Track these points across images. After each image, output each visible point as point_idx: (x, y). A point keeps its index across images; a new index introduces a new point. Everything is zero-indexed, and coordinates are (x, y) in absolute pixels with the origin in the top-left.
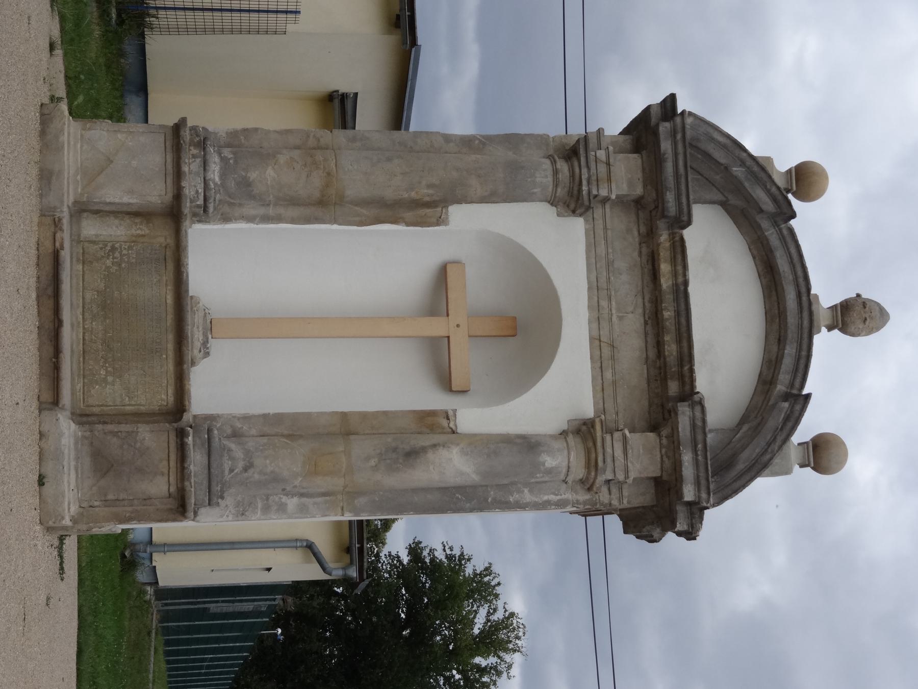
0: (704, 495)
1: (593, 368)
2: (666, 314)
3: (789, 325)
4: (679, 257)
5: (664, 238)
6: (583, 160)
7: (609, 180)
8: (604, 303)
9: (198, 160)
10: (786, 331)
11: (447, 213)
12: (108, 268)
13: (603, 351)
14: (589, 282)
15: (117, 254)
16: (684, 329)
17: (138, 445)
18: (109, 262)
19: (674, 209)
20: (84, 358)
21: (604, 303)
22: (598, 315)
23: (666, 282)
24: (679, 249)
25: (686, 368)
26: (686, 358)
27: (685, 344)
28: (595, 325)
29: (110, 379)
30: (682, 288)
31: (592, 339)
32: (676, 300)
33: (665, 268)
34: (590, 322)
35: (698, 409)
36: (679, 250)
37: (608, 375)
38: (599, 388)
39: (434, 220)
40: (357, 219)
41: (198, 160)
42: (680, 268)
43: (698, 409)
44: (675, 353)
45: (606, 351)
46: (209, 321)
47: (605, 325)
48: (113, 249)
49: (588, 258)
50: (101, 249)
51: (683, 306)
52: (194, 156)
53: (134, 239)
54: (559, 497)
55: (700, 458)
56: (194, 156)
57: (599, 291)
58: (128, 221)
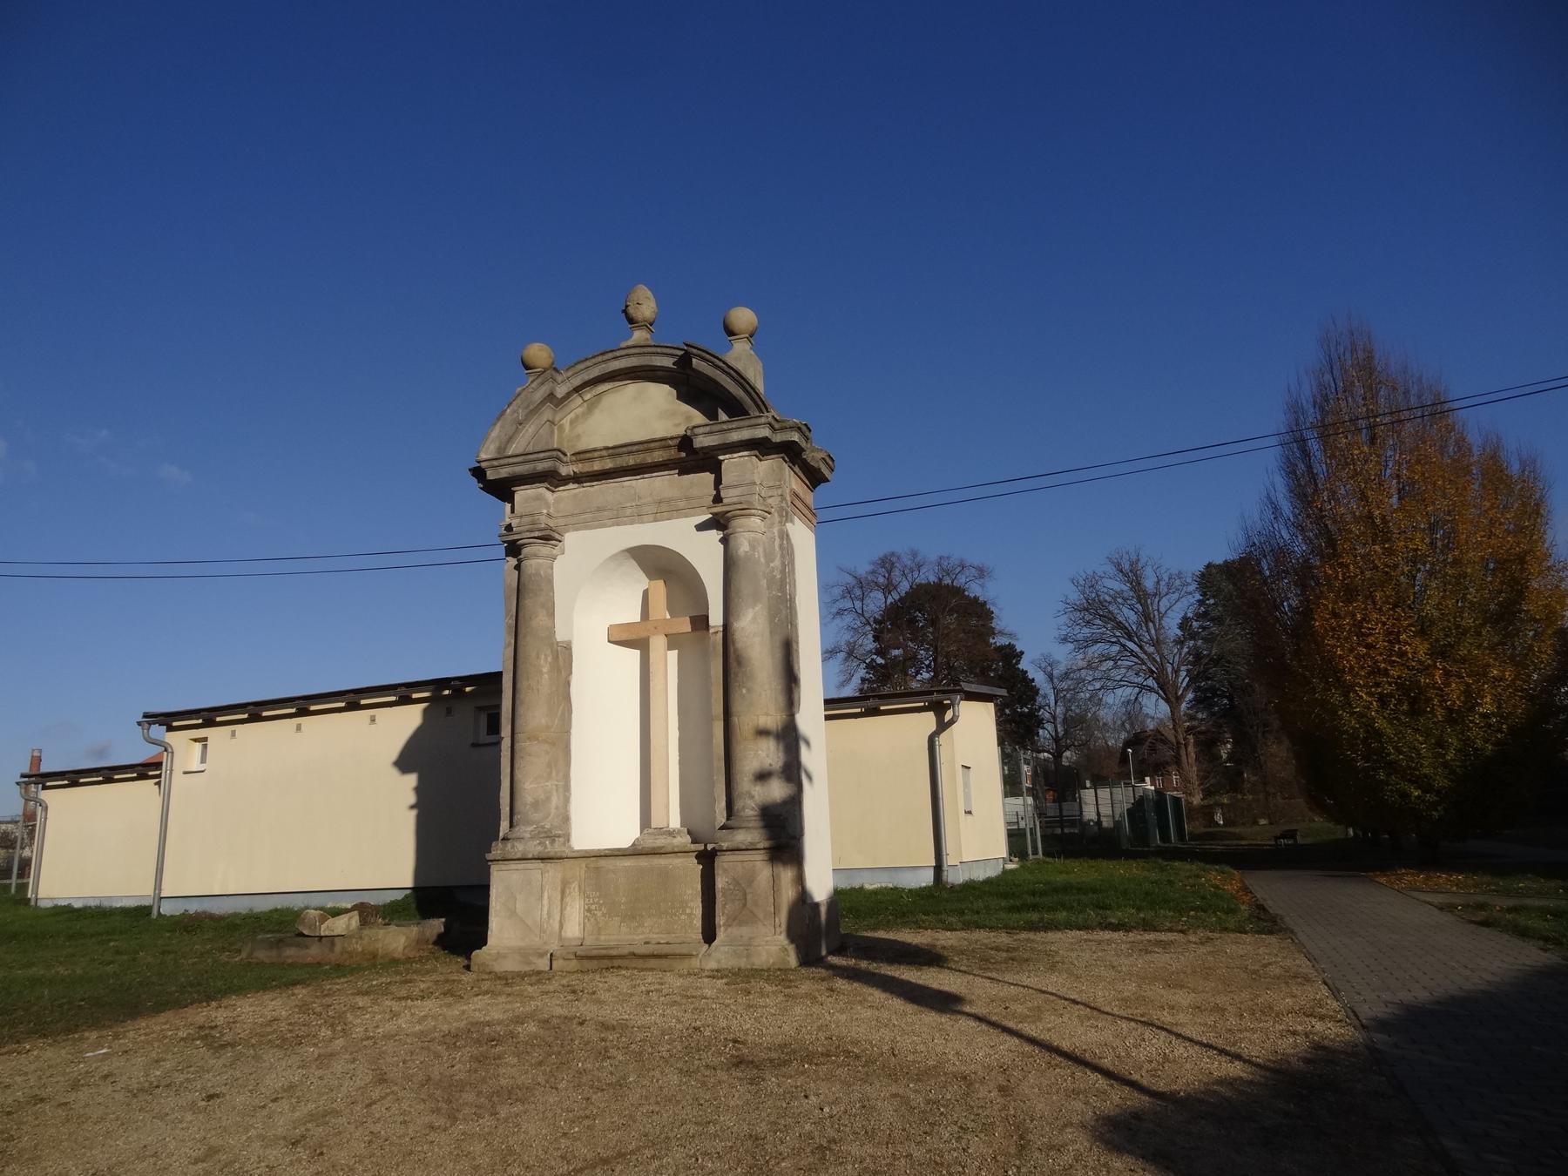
0: (763, 420)
2: (632, 462)
8: (629, 512)
13: (666, 510)
16: (641, 447)
21: (629, 512)
22: (638, 517)
23: (609, 464)
33: (597, 466)
35: (696, 431)
37: (682, 504)
42: (596, 454)
43: (696, 431)
45: (664, 507)
48: (589, 910)
57: (617, 516)
58: (568, 899)
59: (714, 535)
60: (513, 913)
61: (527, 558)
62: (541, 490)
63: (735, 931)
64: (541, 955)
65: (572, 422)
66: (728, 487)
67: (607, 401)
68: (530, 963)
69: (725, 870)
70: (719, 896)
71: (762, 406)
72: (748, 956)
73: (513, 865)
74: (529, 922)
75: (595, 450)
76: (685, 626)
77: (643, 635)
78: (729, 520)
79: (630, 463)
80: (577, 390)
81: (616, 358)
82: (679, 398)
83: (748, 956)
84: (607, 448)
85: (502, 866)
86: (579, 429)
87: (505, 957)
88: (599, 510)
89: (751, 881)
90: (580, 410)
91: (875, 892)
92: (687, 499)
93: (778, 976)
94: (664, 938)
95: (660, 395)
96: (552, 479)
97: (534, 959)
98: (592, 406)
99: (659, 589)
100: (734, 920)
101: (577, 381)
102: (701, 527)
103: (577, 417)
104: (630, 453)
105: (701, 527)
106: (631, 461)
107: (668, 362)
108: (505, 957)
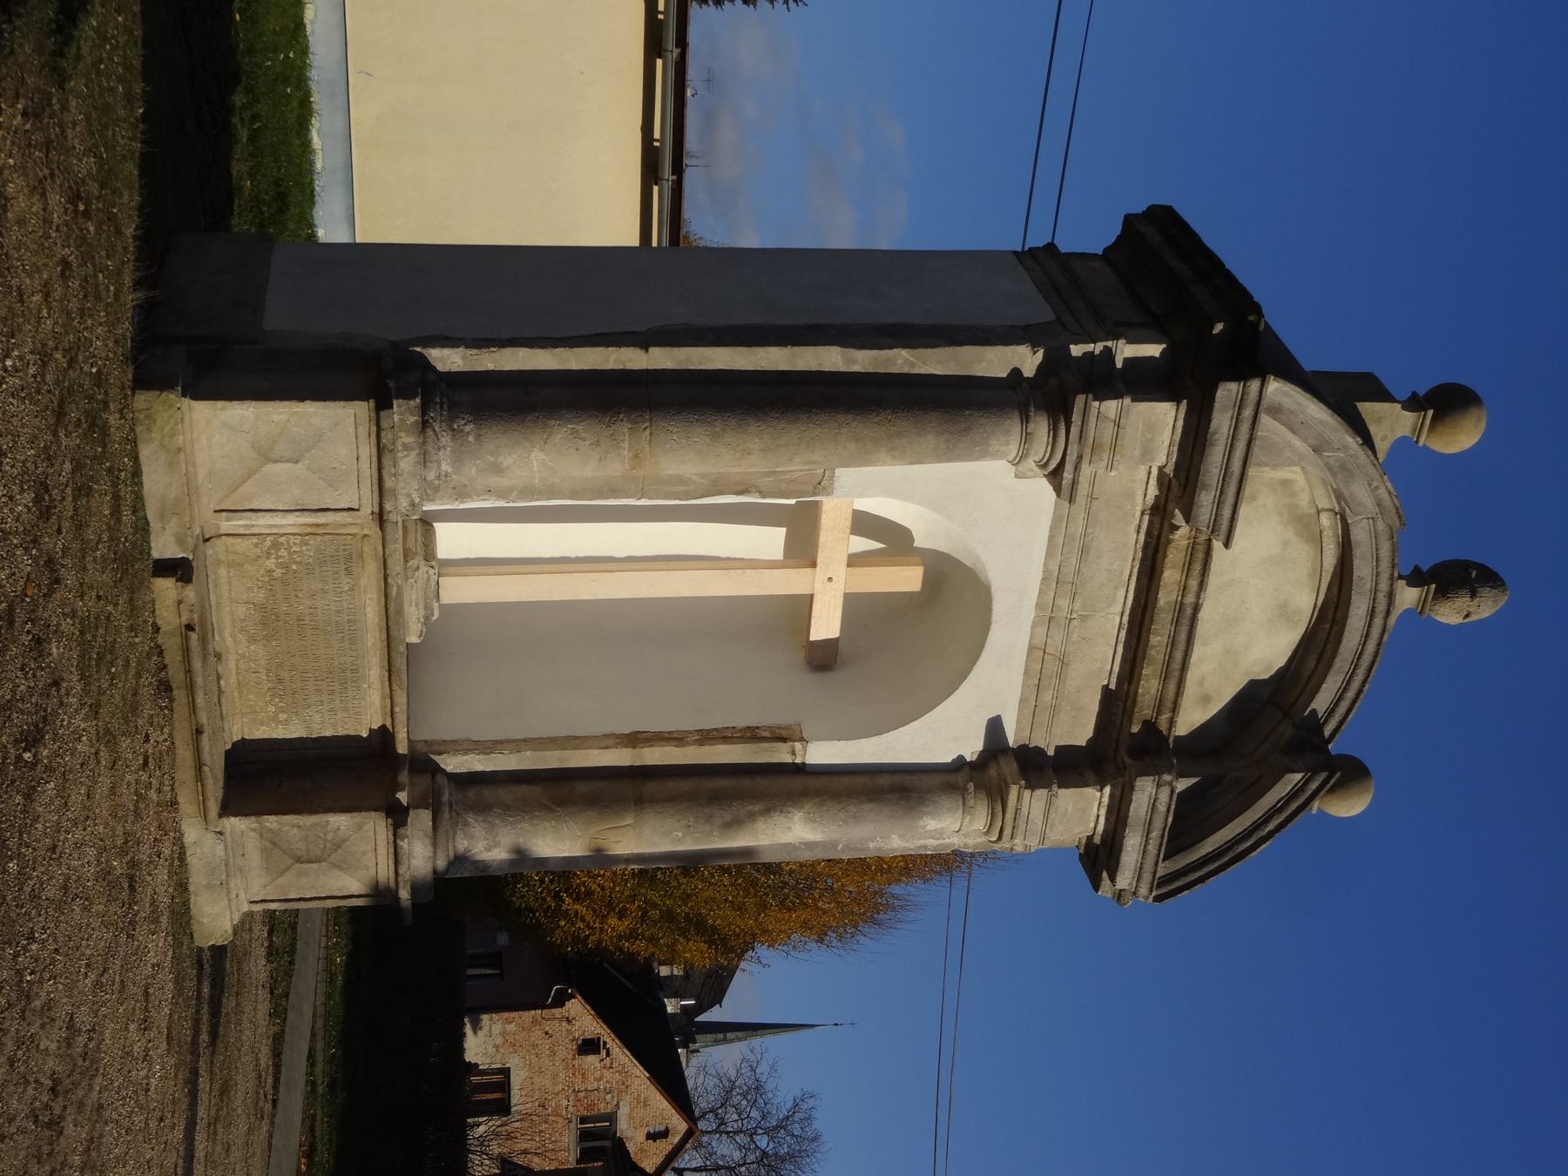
0: (1143, 891)
1: (1024, 685)
2: (1154, 640)
3: (1342, 649)
4: (1197, 567)
5: (1182, 535)
6: (1075, 430)
7: (1114, 448)
8: (1064, 603)
9: (413, 454)
10: (1333, 657)
11: (832, 478)
12: (270, 571)
13: (1045, 667)
14: (1046, 571)
15: (283, 552)
16: (1176, 666)
17: (330, 837)
18: (270, 563)
19: (1207, 517)
20: (240, 693)
21: (1064, 603)
22: (1047, 617)
23: (1166, 596)
24: (1199, 559)
25: (1165, 717)
26: (1169, 704)
27: (1172, 687)
28: (1042, 630)
29: (282, 717)
30: (1189, 611)
31: (1032, 648)
32: (1177, 622)
33: (1171, 576)
34: (1034, 625)
36: (1200, 556)
37: (1047, 697)
38: (1029, 712)
39: (811, 488)
40: (683, 488)
41: (413, 454)
42: (1193, 584)
44: (1153, 691)
45: (1051, 666)
46: (433, 584)
47: (1058, 635)
48: (276, 545)
49: (1051, 538)
50: (256, 545)
51: (1183, 637)
52: (406, 447)
53: (309, 530)
54: (937, 842)
55: (1150, 847)
56: (406, 447)
59: (972, 748)
60: (267, 456)
61: (1027, 437)
63: (252, 844)
64: (180, 541)
65: (1286, 483)
66: (1049, 804)
67: (1302, 555)
68: (162, 517)
69: (360, 827)
70: (307, 820)
72: (209, 887)
73: (367, 451)
74: (248, 487)
75: (1202, 585)
76: (826, 625)
77: (821, 558)
78: (992, 799)
79: (1155, 619)
81: (1372, 613)
82: (1253, 687)
83: (209, 887)
84: (1197, 608)
87: (172, 465)
88: (1084, 550)
90: (1304, 500)
91: (306, 144)
92: (1054, 709)
93: (182, 917)
94: (230, 682)
96: (1180, 487)
97: (172, 525)
98: (1305, 525)
99: (908, 579)
100: (273, 844)
101: (1360, 535)
102: (995, 727)
103: (1294, 494)
104: (1173, 643)
105: (995, 727)
106: (1158, 639)
107: (1321, 703)
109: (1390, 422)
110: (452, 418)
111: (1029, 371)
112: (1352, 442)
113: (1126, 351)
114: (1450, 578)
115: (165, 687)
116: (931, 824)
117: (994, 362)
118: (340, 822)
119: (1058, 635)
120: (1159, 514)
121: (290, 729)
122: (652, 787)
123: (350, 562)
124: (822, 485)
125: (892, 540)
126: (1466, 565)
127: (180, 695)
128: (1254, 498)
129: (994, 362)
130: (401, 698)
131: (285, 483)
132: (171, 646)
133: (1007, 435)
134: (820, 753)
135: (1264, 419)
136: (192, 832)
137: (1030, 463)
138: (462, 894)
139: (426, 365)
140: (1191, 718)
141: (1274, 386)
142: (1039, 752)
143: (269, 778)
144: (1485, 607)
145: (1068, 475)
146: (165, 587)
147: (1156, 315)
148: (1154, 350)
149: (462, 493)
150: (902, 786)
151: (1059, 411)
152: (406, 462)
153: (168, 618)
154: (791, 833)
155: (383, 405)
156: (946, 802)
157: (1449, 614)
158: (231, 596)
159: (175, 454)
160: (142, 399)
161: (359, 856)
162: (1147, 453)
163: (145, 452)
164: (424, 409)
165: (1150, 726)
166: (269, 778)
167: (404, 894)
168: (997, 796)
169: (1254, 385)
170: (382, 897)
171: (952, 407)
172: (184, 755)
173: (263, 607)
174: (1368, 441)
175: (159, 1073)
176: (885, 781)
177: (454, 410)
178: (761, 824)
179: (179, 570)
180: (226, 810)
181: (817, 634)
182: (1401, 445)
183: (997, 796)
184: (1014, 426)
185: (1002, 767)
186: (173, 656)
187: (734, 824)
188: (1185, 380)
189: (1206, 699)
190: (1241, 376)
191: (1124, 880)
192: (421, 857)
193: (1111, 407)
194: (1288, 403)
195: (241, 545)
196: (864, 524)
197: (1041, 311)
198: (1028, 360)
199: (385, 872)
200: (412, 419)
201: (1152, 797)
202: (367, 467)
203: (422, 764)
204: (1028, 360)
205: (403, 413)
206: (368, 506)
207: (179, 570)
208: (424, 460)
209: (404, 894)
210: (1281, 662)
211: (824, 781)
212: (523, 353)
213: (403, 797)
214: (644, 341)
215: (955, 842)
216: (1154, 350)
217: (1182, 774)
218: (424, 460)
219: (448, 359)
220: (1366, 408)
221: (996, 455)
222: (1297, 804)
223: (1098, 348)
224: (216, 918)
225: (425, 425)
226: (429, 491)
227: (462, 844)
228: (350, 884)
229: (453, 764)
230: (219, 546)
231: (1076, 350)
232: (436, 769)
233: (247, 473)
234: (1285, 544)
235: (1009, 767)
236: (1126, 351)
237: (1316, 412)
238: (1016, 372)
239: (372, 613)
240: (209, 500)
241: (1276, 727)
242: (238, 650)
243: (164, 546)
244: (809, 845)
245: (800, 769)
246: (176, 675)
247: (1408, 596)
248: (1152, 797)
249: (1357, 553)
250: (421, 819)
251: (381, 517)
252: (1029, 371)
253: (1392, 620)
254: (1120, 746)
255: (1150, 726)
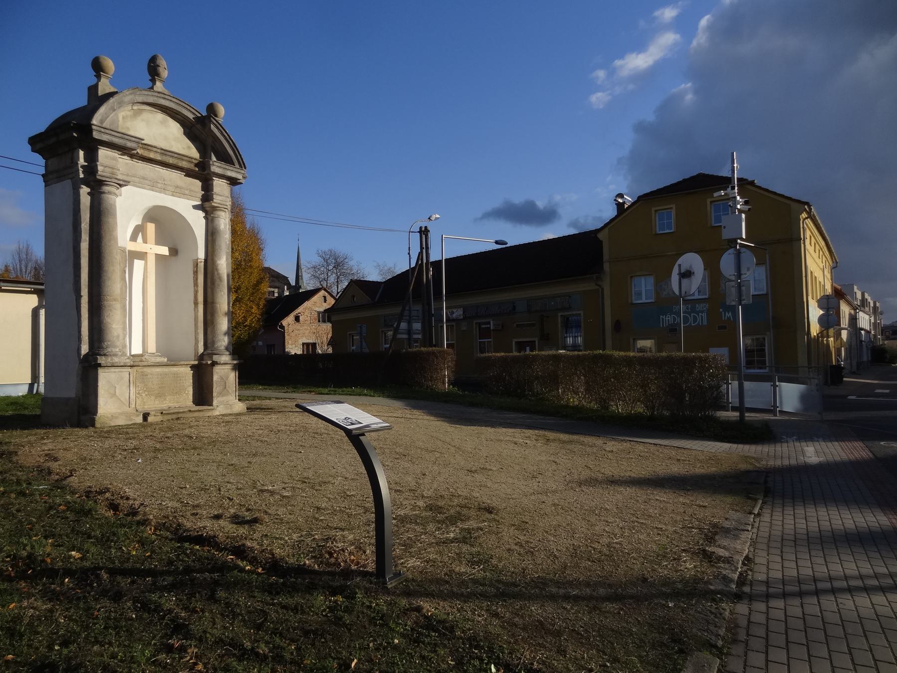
2: (171, 162)
5: (140, 151)
8: (159, 185)
13: (178, 192)
21: (159, 185)
22: (164, 190)
24: (147, 147)
37: (187, 192)
45: (178, 190)
57: (153, 185)
59: (201, 214)
60: (114, 395)
61: (110, 193)
62: (115, 154)
63: (221, 399)
64: (138, 416)
65: (123, 118)
67: (145, 115)
68: (131, 420)
71: (242, 165)
73: (113, 369)
76: (164, 251)
79: (166, 161)
80: (134, 103)
81: (164, 98)
82: (185, 133)
85: (106, 370)
86: (129, 124)
87: (116, 418)
88: (144, 178)
89: (227, 378)
90: (129, 113)
94: (177, 405)
95: (175, 128)
96: (124, 150)
99: (151, 228)
100: (220, 394)
101: (140, 99)
102: (195, 207)
105: (195, 207)
106: (171, 161)
107: (191, 116)
108: (116, 418)
109: (105, 86)
110: (103, 348)
111: (89, 190)
112: (112, 100)
113: (82, 161)
114: (153, 71)
115: (178, 419)
116: (222, 227)
117: (85, 199)
118: (215, 378)
119: (169, 188)
120: (132, 156)
121: (190, 390)
122: (209, 300)
123: (144, 375)
124: (123, 250)
125: (139, 230)
126: (149, 67)
127: (180, 415)
128: (128, 128)
129: (85, 199)
130: (182, 363)
131: (122, 391)
132: (166, 418)
133: (108, 198)
134: (201, 255)
135: (104, 125)
136: (217, 413)
137: (117, 192)
138: (237, 349)
139: (86, 355)
140: (194, 153)
141: (95, 121)
142: (203, 196)
143: (203, 394)
144: (162, 63)
145: (121, 183)
146: (150, 419)
147: (68, 146)
148: (81, 153)
149: (124, 346)
150: (211, 234)
151: (101, 183)
152: (116, 360)
153: (159, 418)
154: (224, 264)
155: (100, 365)
156: (216, 221)
157: (164, 74)
158: (153, 405)
159: (113, 417)
160: (98, 425)
161: (225, 374)
162: (114, 159)
163: (113, 424)
164: (100, 355)
165: (196, 165)
166: (203, 394)
167: (235, 362)
168: (215, 209)
169: (94, 127)
170: (235, 368)
171: (100, 215)
172: (196, 414)
173: (156, 397)
174: (111, 95)
175: (274, 416)
176: (210, 238)
177: (100, 347)
178: (220, 272)
179: (146, 416)
180: (211, 405)
181: (167, 253)
182: (112, 83)
183: (215, 209)
184: (105, 196)
185: (206, 204)
186: (170, 417)
187: (220, 279)
188: (92, 147)
189: (189, 147)
190: (91, 131)
191: (240, 176)
192: (226, 358)
193: (100, 168)
194: (100, 118)
195: (138, 402)
196: (134, 238)
197: (68, 183)
198: (84, 190)
199: (229, 367)
200: (103, 358)
201: (216, 167)
202: (117, 370)
203: (201, 357)
204: (84, 190)
205: (101, 360)
206: (129, 370)
207: (146, 416)
208: (116, 355)
209: (235, 362)
210: (178, 125)
211: (209, 254)
212: (83, 329)
213: (209, 362)
214: (79, 297)
215: (228, 220)
216: (81, 153)
217: (211, 158)
218: (116, 355)
219: (85, 349)
220: (100, 93)
221: (115, 202)
222: (220, 127)
223: (81, 170)
224: (239, 407)
225: (105, 355)
226: (124, 354)
227: (223, 348)
228: (233, 377)
229: (201, 350)
230: (138, 408)
231: (82, 176)
232: (202, 354)
233: (117, 399)
234: (142, 120)
235: (207, 204)
236: (82, 161)
237: (102, 110)
238: (89, 194)
239: (158, 370)
240: (127, 409)
241: (198, 129)
242: (169, 403)
243: (140, 420)
244: (227, 259)
245: (206, 261)
246: (175, 416)
247: (159, 86)
248: (216, 167)
249: (145, 101)
250: (216, 358)
251: (131, 366)
252: (89, 190)
253: (166, 92)
254: (201, 173)
255: (196, 165)
